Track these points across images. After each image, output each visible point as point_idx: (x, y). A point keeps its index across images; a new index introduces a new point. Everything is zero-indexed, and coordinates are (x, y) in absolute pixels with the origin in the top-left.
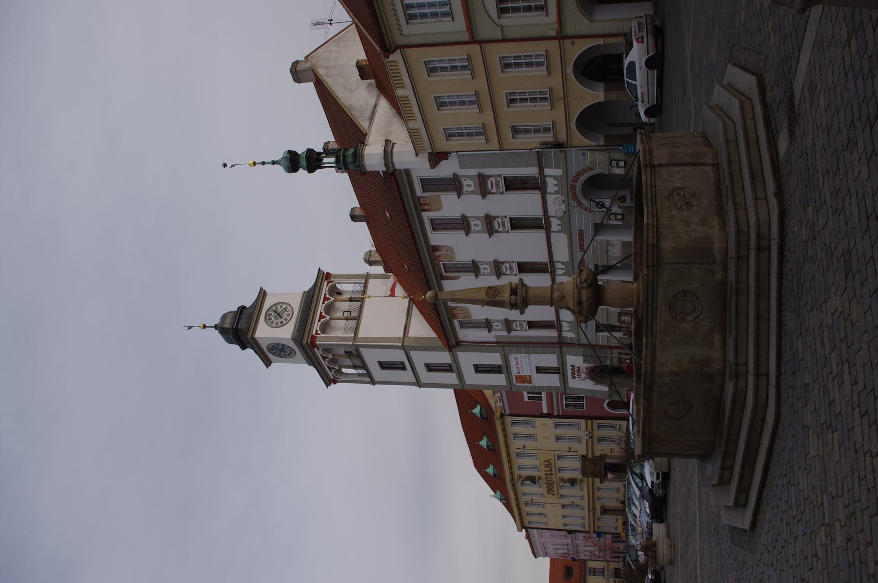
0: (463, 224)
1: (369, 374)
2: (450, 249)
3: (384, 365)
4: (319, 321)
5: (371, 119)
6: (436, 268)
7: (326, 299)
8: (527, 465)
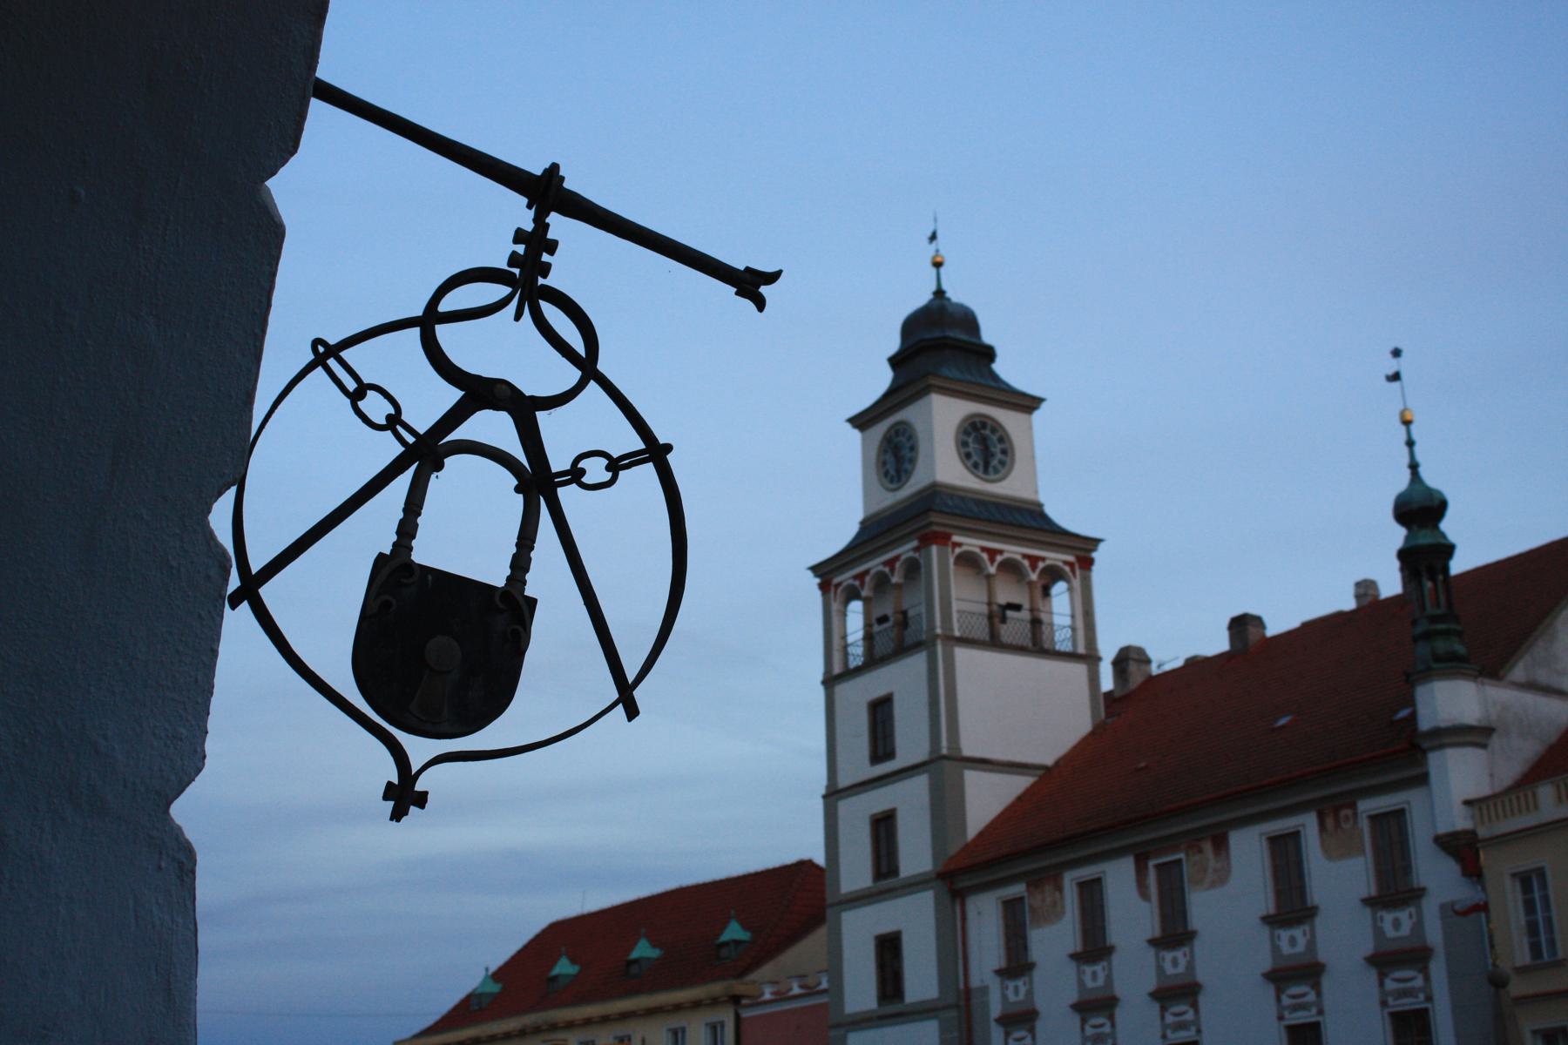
1: (849, 674)
2: (1222, 878)
3: (881, 710)
4: (984, 549)
5: (1531, 686)
6: (1169, 844)
7: (1034, 560)
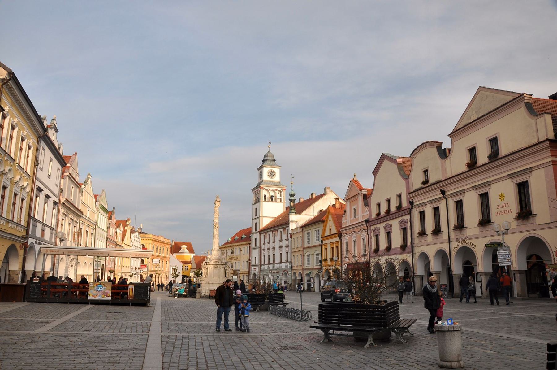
0: (281, 240)
8: (237, 251)
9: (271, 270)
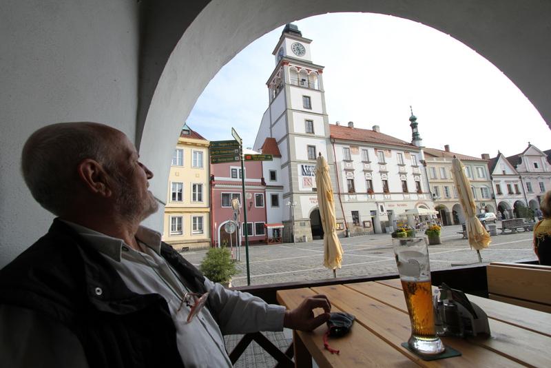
6: (382, 148)
9: (383, 202)
